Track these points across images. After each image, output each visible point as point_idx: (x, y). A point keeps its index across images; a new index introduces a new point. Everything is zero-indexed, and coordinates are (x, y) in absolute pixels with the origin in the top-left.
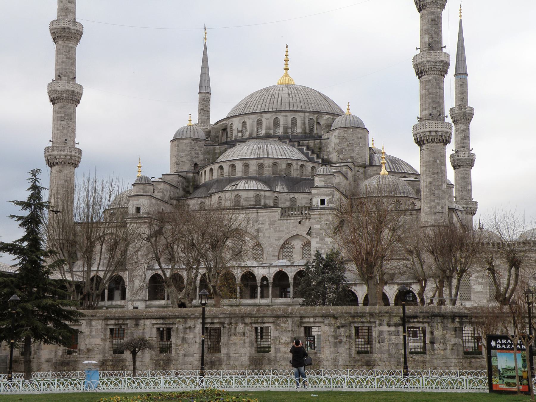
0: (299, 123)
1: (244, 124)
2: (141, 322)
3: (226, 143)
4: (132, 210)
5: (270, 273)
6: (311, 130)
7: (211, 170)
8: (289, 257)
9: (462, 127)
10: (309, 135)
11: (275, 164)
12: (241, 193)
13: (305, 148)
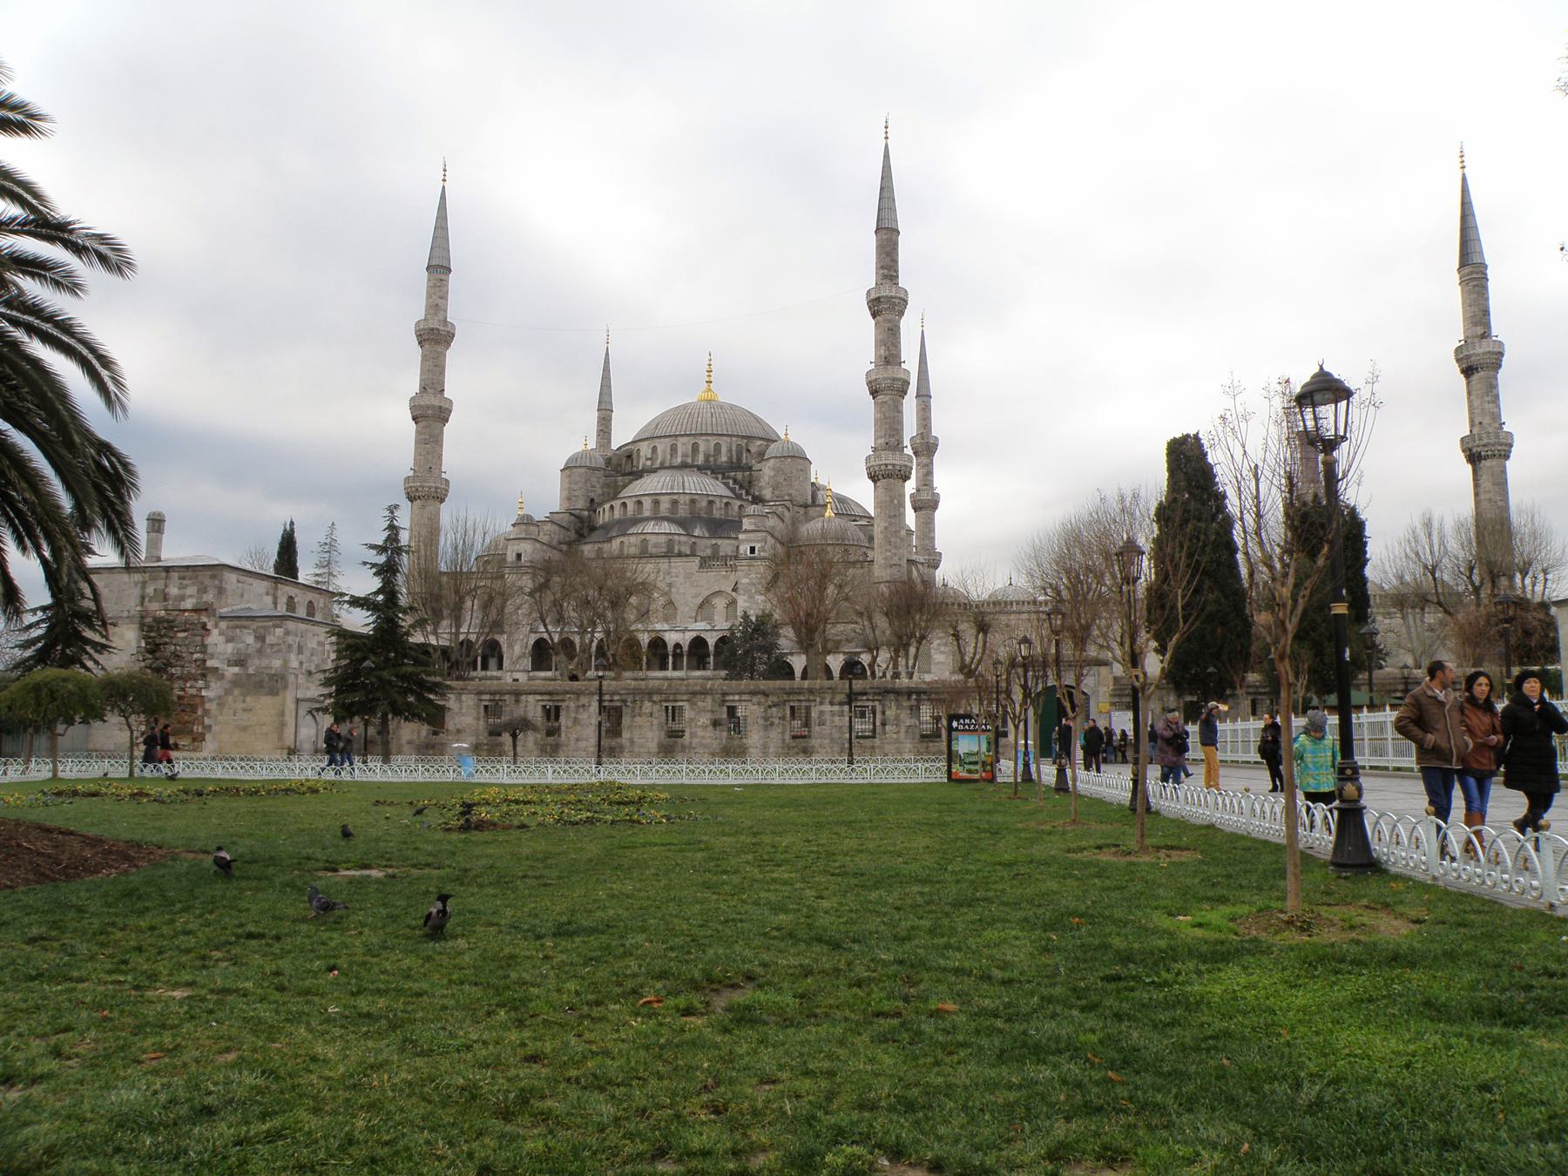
0: (724, 450)
1: (654, 449)
2: (523, 698)
3: (631, 473)
4: (511, 557)
5: (685, 639)
6: (739, 459)
8: (709, 619)
9: (924, 460)
10: (736, 465)
11: (693, 501)
12: (648, 537)
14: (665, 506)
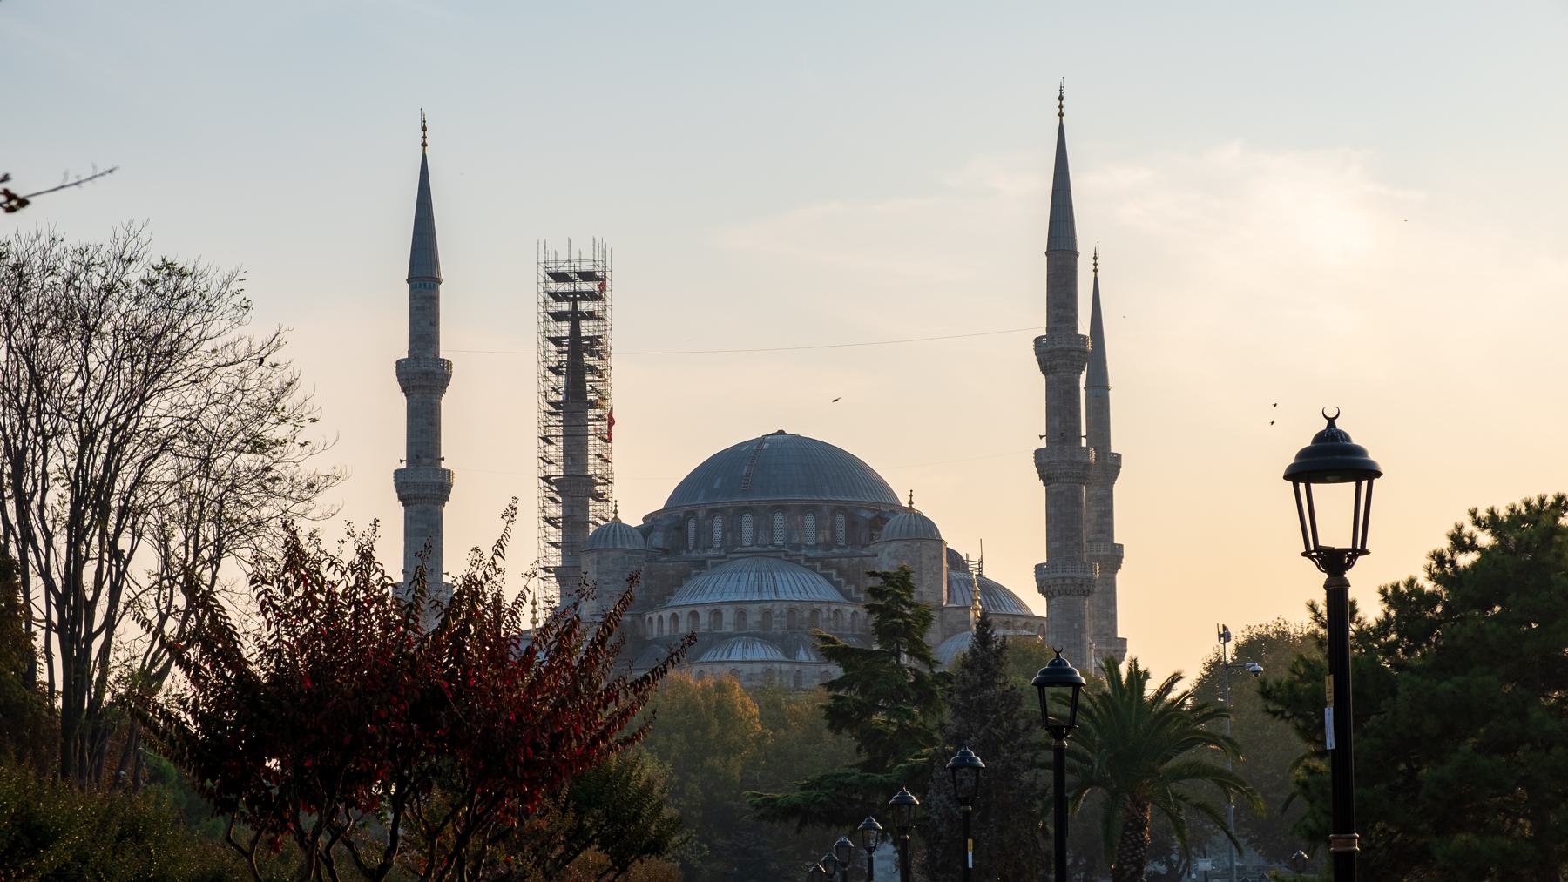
7: (675, 617)
11: (792, 611)
13: (834, 573)
14: (754, 618)
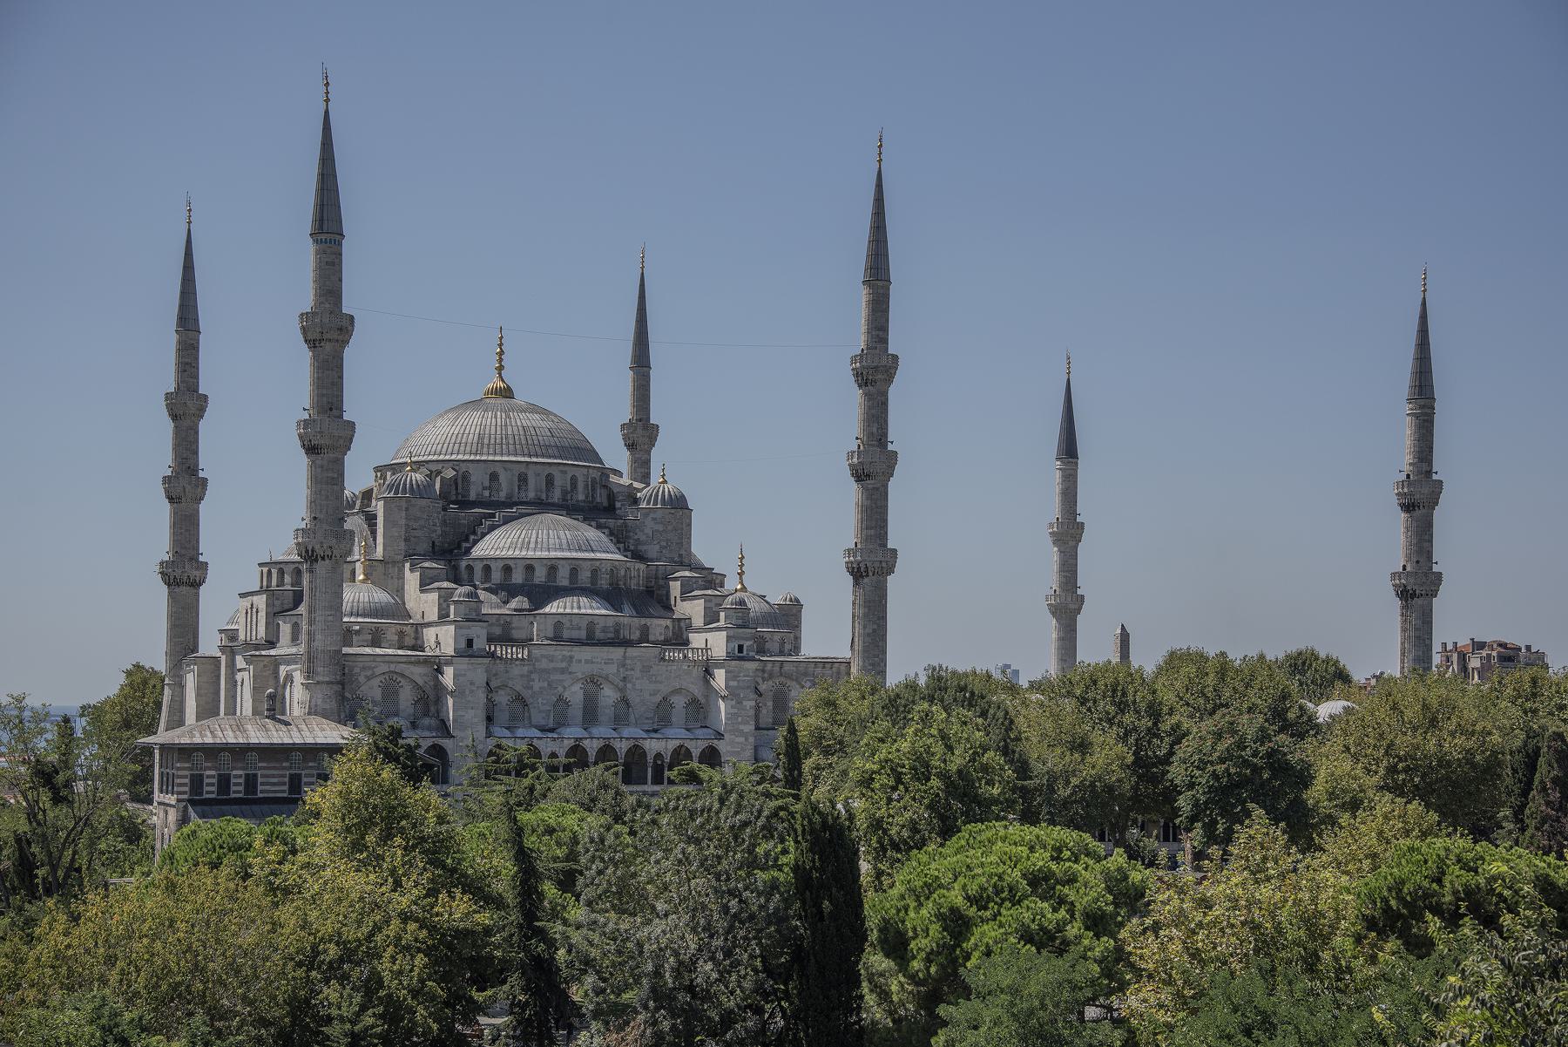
0: (580, 486)
